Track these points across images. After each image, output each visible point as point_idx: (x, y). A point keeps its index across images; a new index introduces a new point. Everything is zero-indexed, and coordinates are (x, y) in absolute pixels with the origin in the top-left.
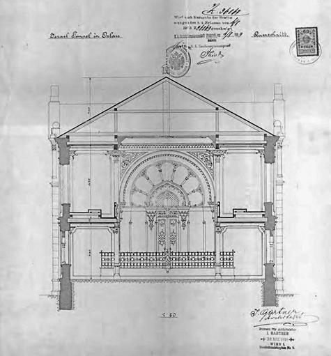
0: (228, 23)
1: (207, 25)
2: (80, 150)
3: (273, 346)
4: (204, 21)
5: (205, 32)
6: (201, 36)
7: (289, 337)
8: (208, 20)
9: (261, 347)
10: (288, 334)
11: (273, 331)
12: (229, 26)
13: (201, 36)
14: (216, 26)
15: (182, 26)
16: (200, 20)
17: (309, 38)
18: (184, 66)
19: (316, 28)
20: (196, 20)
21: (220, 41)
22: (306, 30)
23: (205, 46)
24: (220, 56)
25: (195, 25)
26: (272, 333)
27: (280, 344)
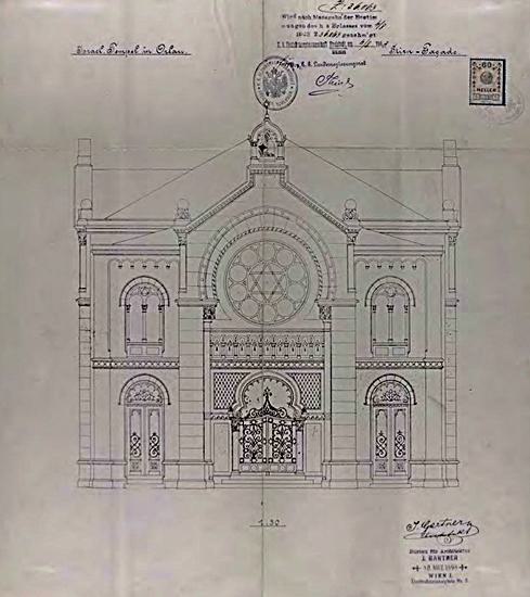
0: (370, 26)
1: (333, 31)
3: (433, 579)
4: (330, 22)
5: (328, 39)
6: (323, 45)
7: (458, 563)
8: (338, 22)
10: (456, 558)
11: (433, 555)
12: (371, 31)
13: (323, 45)
14: (350, 31)
15: (296, 31)
16: (324, 22)
17: (491, 76)
18: (287, 92)
19: (504, 61)
20: (315, 22)
21: (351, 55)
22: (487, 62)
23: (325, 64)
24: (348, 85)
25: (315, 30)
26: (430, 559)
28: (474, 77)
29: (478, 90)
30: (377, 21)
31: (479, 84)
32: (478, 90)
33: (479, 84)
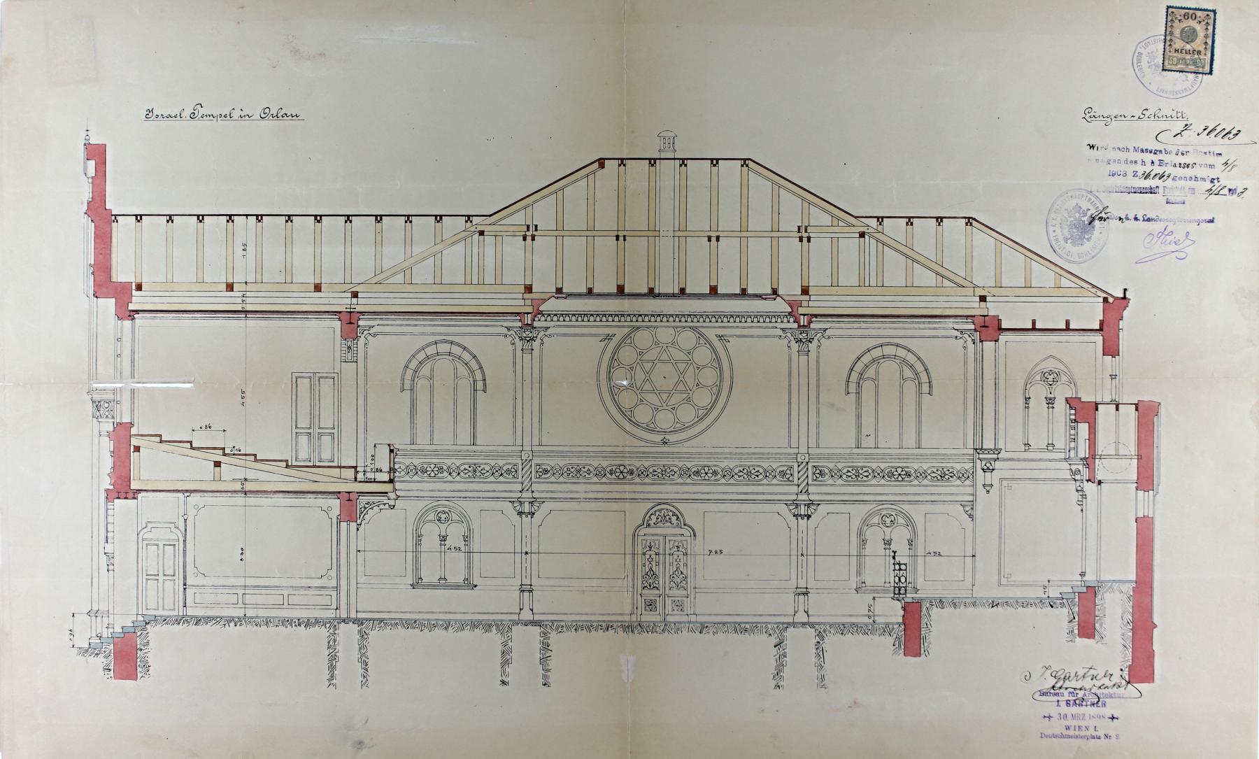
0: (1211, 166)
2: (834, 328)
4: (1156, 158)
9: (1043, 736)
27: (1087, 728)
28: (1171, 34)
29: (1176, 51)
30: (1222, 159)
31: (1179, 44)
32: (1176, 51)
33: (1179, 44)
